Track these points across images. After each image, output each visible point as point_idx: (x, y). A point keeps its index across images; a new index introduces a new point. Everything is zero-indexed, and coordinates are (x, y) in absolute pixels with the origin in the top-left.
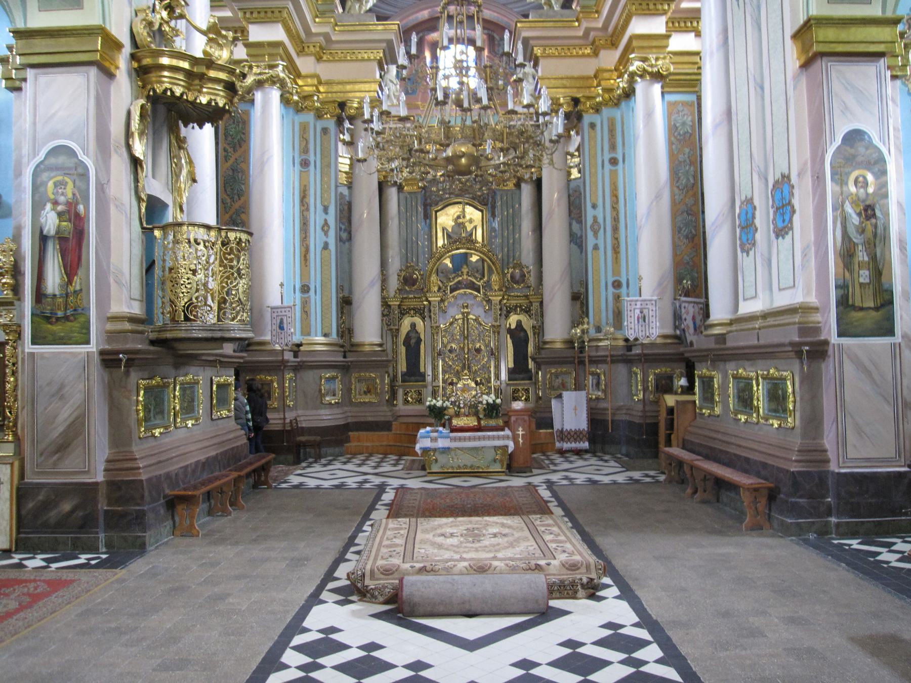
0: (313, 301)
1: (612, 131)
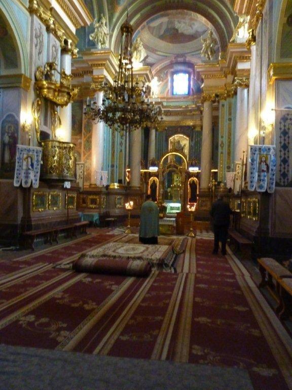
0: (115, 171)
1: (230, 108)
